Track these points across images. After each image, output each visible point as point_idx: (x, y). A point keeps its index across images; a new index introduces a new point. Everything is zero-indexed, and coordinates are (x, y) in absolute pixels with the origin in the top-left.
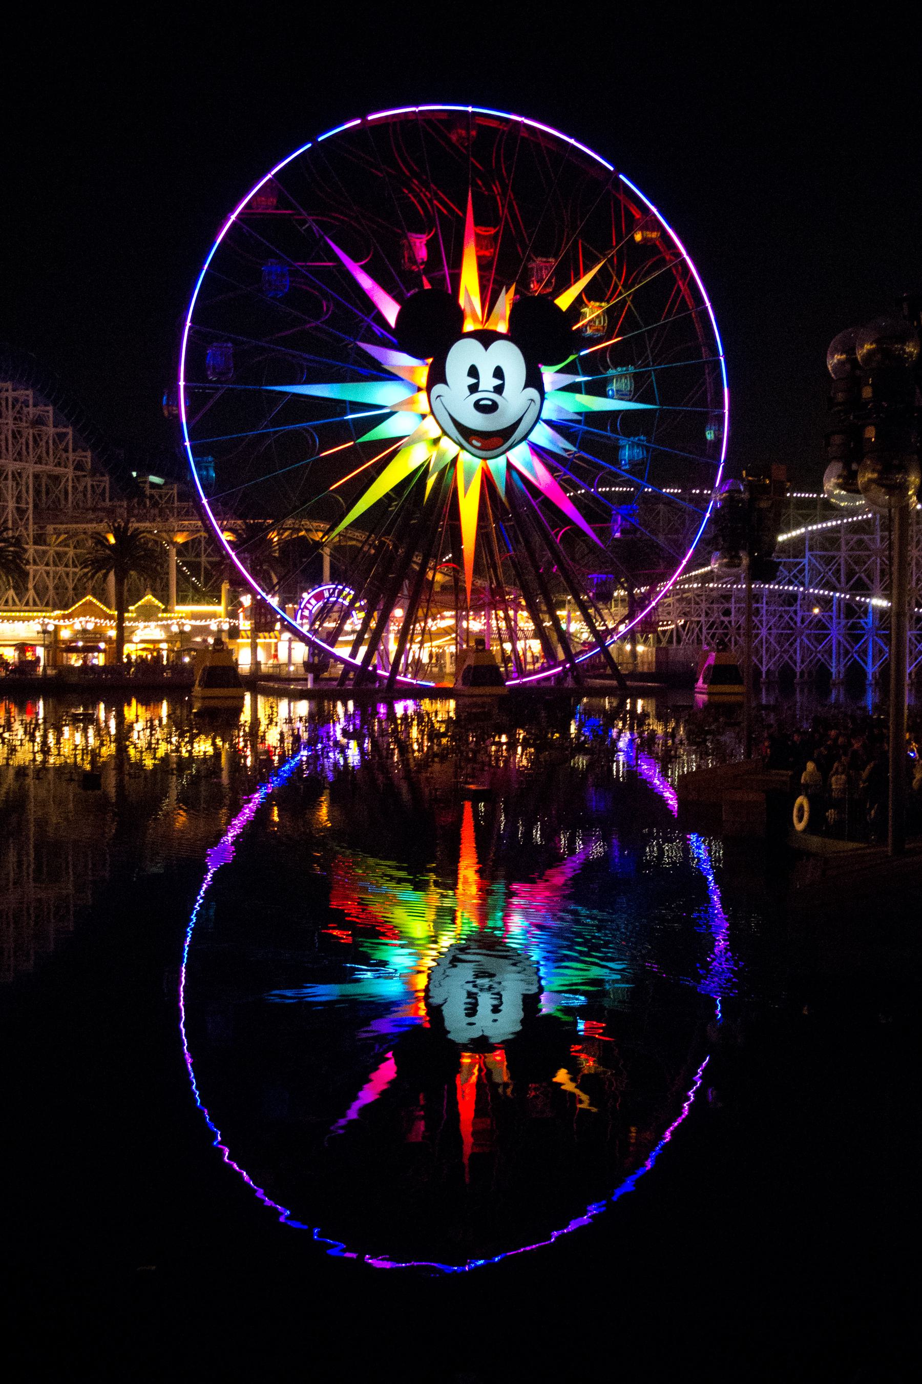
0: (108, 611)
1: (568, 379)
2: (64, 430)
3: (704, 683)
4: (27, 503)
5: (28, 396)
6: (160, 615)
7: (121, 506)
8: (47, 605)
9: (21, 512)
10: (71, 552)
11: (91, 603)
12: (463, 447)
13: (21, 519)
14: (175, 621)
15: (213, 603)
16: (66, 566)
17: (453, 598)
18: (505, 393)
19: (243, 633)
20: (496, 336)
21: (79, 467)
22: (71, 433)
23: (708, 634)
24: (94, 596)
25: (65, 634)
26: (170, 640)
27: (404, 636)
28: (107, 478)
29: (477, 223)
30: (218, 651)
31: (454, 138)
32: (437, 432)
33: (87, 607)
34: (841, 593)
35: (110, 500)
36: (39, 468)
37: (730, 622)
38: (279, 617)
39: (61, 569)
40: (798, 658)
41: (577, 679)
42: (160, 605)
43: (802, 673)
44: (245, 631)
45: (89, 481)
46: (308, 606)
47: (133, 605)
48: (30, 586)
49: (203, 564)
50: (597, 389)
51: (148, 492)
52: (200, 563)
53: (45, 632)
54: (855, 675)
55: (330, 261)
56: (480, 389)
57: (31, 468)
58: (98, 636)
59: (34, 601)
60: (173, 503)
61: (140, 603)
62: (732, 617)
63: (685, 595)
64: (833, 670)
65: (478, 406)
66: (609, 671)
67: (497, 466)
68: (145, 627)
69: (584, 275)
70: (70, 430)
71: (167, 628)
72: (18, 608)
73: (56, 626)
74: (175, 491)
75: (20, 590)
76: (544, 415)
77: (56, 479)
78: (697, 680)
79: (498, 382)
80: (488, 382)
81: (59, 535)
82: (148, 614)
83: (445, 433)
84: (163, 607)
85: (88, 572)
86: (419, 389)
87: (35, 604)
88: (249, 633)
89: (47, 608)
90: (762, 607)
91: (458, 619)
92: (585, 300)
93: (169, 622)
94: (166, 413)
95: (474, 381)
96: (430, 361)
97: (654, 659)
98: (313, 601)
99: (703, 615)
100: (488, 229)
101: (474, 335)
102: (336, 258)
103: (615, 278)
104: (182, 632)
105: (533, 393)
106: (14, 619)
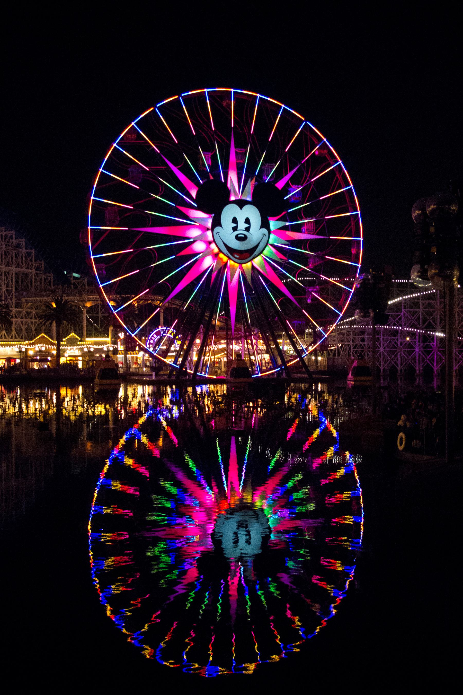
0: (52, 341)
1: (282, 224)
2: (31, 251)
3: (352, 375)
4: (12, 287)
6: (78, 343)
7: (59, 289)
8: (22, 338)
9: (9, 292)
10: (34, 312)
11: (44, 337)
12: (229, 258)
13: (9, 295)
14: (85, 346)
15: (105, 337)
16: (31, 318)
17: (225, 333)
18: (250, 231)
19: (120, 352)
20: (246, 203)
21: (38, 269)
22: (34, 252)
23: (354, 351)
24: (45, 333)
25: (31, 353)
26: (84, 355)
27: (201, 353)
28: (52, 275)
29: (236, 147)
30: (108, 361)
31: (224, 104)
32: (216, 250)
33: (41, 339)
34: (420, 330)
35: (54, 285)
36: (18, 269)
37: (364, 345)
38: (138, 343)
39: (29, 320)
40: (399, 364)
41: (288, 374)
42: (78, 338)
43: (401, 370)
44: (121, 351)
45: (43, 276)
46: (153, 338)
47: (65, 338)
48: (13, 328)
49: (100, 318)
51: (72, 282)
52: (98, 317)
53: (21, 352)
54: (428, 371)
55: (163, 166)
56: (238, 229)
57: (14, 270)
58: (47, 354)
59: (15, 336)
60: (85, 287)
61: (68, 337)
62: (366, 343)
63: (341, 332)
64: (417, 369)
65: (237, 238)
66: (304, 370)
67: (247, 266)
68: (71, 349)
69: (290, 171)
70: (33, 251)
71: (82, 349)
72: (7, 340)
73: (26, 349)
74: (86, 281)
75: (8, 331)
76: (271, 242)
77: (26, 275)
78: (348, 374)
79: (248, 225)
80: (242, 225)
81: (27, 302)
82: (72, 342)
83: (220, 251)
84: (80, 339)
85: (43, 321)
86: (208, 229)
87: (16, 338)
88: (123, 352)
89: (21, 340)
90: (381, 337)
91: (228, 344)
92: (290, 184)
93: (83, 346)
94: (81, 242)
95: (235, 225)
96: (213, 215)
97: (326, 364)
98: (155, 336)
99: (351, 341)
100: (242, 149)
101: (235, 202)
102: (166, 165)
103: (305, 173)
104: (89, 351)
105: (264, 231)
106: (5, 345)
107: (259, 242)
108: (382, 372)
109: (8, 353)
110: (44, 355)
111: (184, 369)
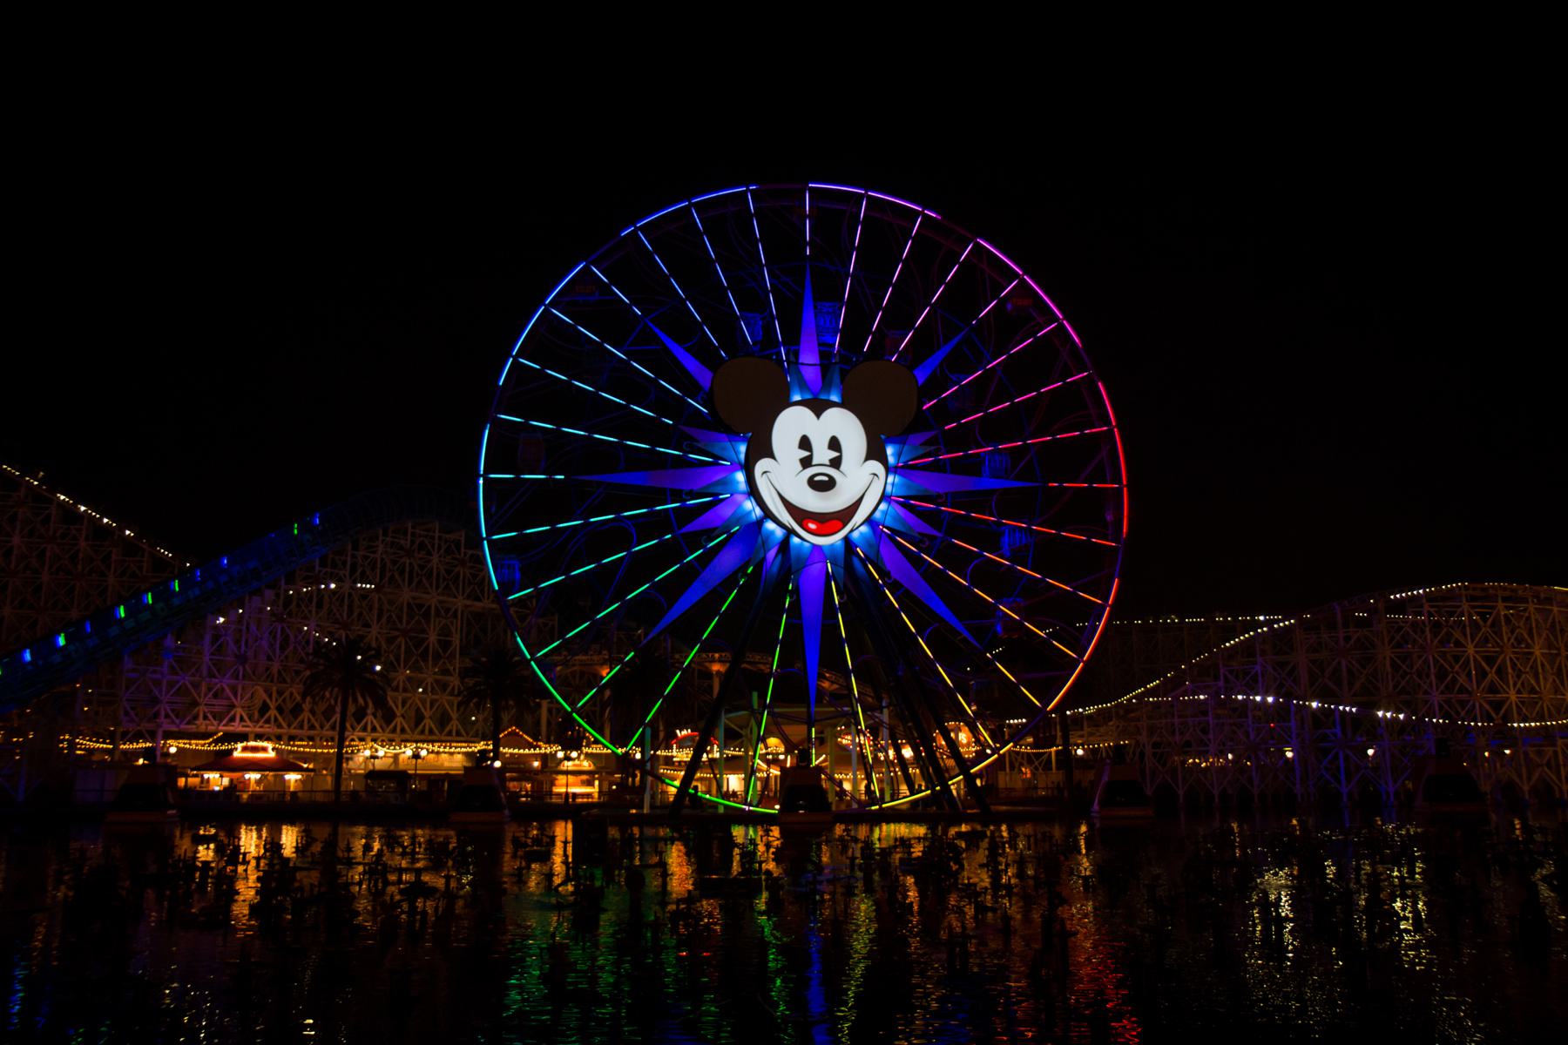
8: (476, 735)
17: (805, 710)
18: (842, 468)
23: (1154, 755)
32: (758, 512)
57: (460, 602)
87: (458, 734)
105: (876, 466)
107: (861, 494)
108: (1217, 800)
109: (442, 764)
111: (691, 791)
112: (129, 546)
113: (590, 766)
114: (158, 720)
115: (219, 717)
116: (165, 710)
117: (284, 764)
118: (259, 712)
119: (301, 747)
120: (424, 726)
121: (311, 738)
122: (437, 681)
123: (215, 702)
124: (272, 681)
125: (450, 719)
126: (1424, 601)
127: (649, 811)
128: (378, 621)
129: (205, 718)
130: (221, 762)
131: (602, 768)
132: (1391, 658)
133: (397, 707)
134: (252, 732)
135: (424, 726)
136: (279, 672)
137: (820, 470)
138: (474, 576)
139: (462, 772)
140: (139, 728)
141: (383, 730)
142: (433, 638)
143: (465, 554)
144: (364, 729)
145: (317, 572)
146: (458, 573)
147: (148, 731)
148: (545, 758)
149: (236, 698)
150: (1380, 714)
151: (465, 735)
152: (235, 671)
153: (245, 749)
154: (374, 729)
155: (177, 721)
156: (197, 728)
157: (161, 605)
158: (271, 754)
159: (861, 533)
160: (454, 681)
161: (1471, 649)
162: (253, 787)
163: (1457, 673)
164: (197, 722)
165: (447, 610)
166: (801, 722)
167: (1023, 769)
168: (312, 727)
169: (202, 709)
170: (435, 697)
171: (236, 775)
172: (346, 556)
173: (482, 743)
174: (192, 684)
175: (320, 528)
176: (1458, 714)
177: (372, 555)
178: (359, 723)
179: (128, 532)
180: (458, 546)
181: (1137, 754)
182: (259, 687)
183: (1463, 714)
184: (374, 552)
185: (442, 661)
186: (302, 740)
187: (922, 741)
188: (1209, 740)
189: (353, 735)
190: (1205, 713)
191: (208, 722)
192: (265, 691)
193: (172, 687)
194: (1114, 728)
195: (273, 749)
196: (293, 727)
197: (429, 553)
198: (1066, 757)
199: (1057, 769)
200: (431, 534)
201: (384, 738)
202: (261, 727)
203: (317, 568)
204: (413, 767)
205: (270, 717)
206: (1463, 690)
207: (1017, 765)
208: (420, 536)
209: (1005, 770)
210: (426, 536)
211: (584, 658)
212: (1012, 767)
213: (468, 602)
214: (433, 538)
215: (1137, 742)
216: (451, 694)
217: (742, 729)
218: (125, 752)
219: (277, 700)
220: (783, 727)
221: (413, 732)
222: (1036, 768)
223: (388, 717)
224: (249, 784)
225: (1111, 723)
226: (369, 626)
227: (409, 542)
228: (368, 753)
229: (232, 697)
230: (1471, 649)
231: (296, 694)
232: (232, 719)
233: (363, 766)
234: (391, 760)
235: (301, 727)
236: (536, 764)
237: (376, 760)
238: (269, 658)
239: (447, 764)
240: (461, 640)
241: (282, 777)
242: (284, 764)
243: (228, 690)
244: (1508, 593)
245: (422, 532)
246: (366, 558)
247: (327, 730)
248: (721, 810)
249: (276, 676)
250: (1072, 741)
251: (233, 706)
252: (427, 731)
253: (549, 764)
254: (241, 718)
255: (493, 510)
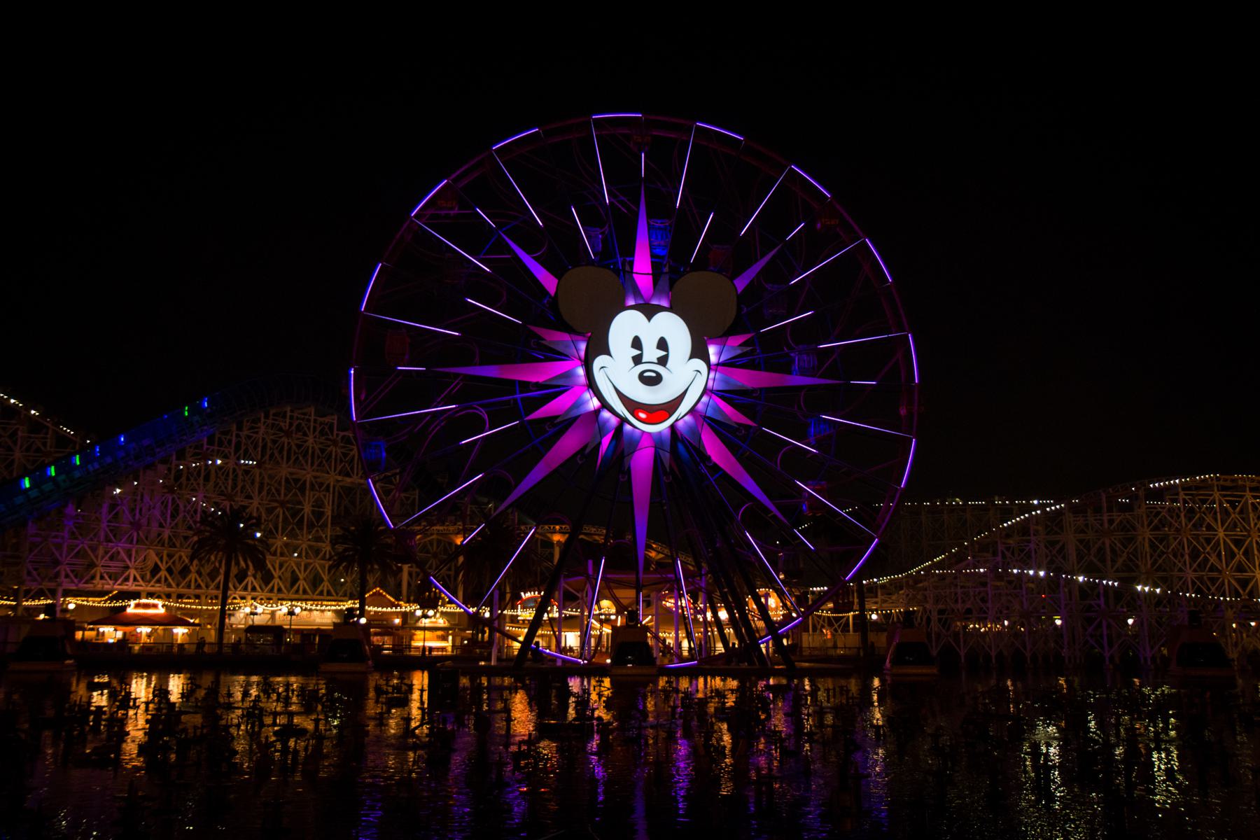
5: (334, 420)
8: (345, 595)
17: (634, 576)
23: (940, 620)
29: (649, 216)
50: (785, 368)
56: (643, 361)
57: (332, 478)
80: (651, 353)
87: (329, 593)
95: (637, 352)
105: (699, 364)
108: (994, 661)
109: (315, 620)
110: (379, 624)
112: (34, 425)
113: (445, 623)
114: (58, 580)
115: (114, 577)
116: (65, 570)
117: (173, 620)
118: (151, 572)
119: (189, 604)
120: (299, 587)
121: (197, 597)
122: (310, 547)
123: (111, 564)
124: (163, 545)
125: (322, 580)
126: (1180, 490)
127: (496, 664)
128: (260, 492)
129: (102, 578)
130: (115, 617)
131: (454, 625)
132: (1150, 540)
133: (275, 569)
134: (143, 591)
135: (299, 587)
136: (170, 537)
137: (649, 366)
138: (345, 455)
139: (332, 627)
140: (41, 587)
141: (262, 590)
142: (307, 509)
143: (337, 435)
144: (245, 589)
145: (205, 449)
146: (331, 452)
147: (50, 590)
148: (405, 616)
149: (130, 560)
150: (1139, 588)
151: (335, 595)
152: (130, 536)
153: (137, 606)
154: (254, 589)
155: (76, 580)
156: (95, 586)
157: (63, 477)
158: (161, 611)
159: (685, 422)
160: (326, 547)
161: (1221, 534)
162: (144, 639)
163: (1208, 553)
164: (94, 582)
165: (321, 485)
166: (630, 587)
167: (824, 631)
168: (199, 587)
169: (99, 570)
170: (308, 561)
171: (129, 629)
172: (232, 435)
173: (350, 602)
174: (90, 547)
175: (209, 410)
176: (1209, 589)
177: (255, 435)
178: (240, 583)
179: (33, 412)
180: (331, 428)
181: (924, 619)
182: (151, 551)
183: (1213, 589)
184: (257, 433)
185: (316, 529)
186: (189, 598)
187: (735, 606)
188: (988, 608)
189: (235, 594)
190: (984, 585)
191: (103, 581)
192: (157, 555)
193: (73, 550)
194: (904, 597)
195: (163, 606)
196: (181, 586)
197: (305, 434)
198: (862, 622)
199: (855, 631)
200: (307, 417)
201: (262, 597)
202: (153, 586)
203: (205, 446)
204: (289, 622)
205: (160, 577)
206: (1213, 568)
207: (819, 627)
208: (298, 418)
209: (808, 631)
210: (303, 419)
211: (441, 528)
212: (815, 629)
213: (340, 478)
214: (309, 420)
215: (925, 609)
216: (323, 558)
217: (578, 592)
218: (27, 608)
219: (167, 563)
220: (615, 591)
221: (289, 591)
222: (836, 630)
223: (267, 578)
224: (141, 636)
225: (901, 592)
226: (252, 498)
227: (287, 424)
228: (248, 610)
229: (127, 560)
230: (1221, 534)
231: (184, 557)
232: (127, 579)
233: (243, 622)
234: (269, 616)
235: (189, 587)
236: (397, 621)
237: (255, 616)
238: (161, 526)
239: (318, 620)
240: (333, 511)
241: (171, 630)
242: (173, 620)
243: (123, 554)
244: (1255, 484)
245: (299, 416)
246: (249, 437)
247: (212, 589)
248: (559, 663)
249: (166, 542)
250: (867, 607)
251: (127, 567)
252: (301, 591)
253: (409, 621)
254: (135, 579)
255: (363, 397)
